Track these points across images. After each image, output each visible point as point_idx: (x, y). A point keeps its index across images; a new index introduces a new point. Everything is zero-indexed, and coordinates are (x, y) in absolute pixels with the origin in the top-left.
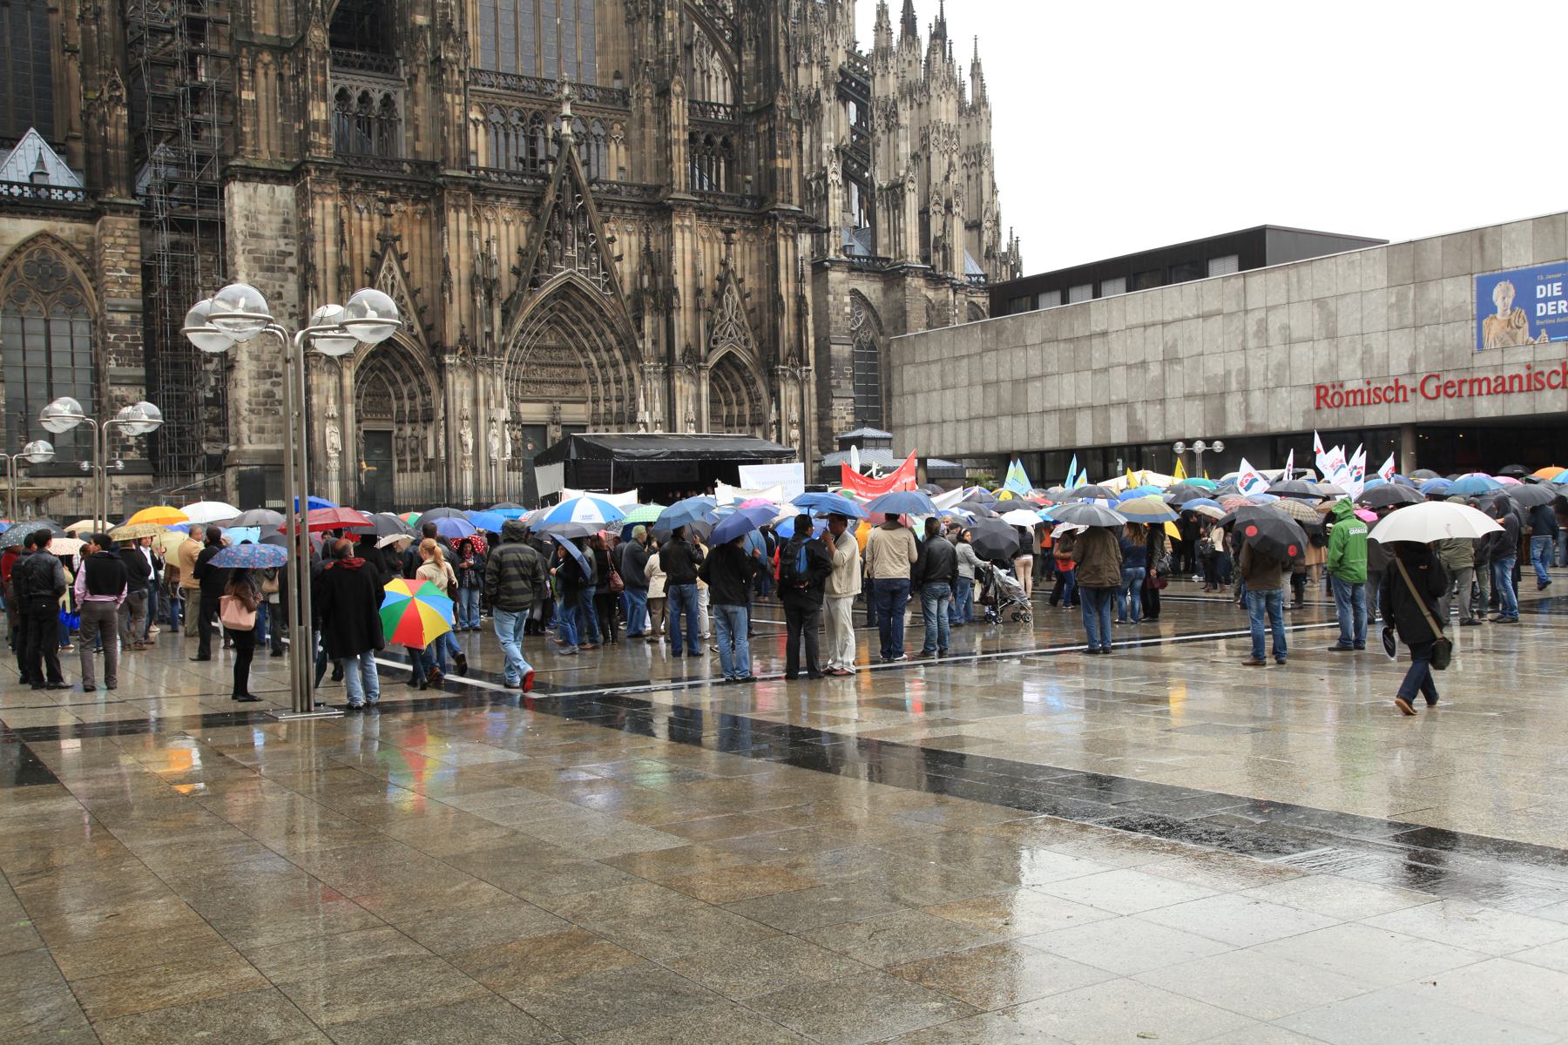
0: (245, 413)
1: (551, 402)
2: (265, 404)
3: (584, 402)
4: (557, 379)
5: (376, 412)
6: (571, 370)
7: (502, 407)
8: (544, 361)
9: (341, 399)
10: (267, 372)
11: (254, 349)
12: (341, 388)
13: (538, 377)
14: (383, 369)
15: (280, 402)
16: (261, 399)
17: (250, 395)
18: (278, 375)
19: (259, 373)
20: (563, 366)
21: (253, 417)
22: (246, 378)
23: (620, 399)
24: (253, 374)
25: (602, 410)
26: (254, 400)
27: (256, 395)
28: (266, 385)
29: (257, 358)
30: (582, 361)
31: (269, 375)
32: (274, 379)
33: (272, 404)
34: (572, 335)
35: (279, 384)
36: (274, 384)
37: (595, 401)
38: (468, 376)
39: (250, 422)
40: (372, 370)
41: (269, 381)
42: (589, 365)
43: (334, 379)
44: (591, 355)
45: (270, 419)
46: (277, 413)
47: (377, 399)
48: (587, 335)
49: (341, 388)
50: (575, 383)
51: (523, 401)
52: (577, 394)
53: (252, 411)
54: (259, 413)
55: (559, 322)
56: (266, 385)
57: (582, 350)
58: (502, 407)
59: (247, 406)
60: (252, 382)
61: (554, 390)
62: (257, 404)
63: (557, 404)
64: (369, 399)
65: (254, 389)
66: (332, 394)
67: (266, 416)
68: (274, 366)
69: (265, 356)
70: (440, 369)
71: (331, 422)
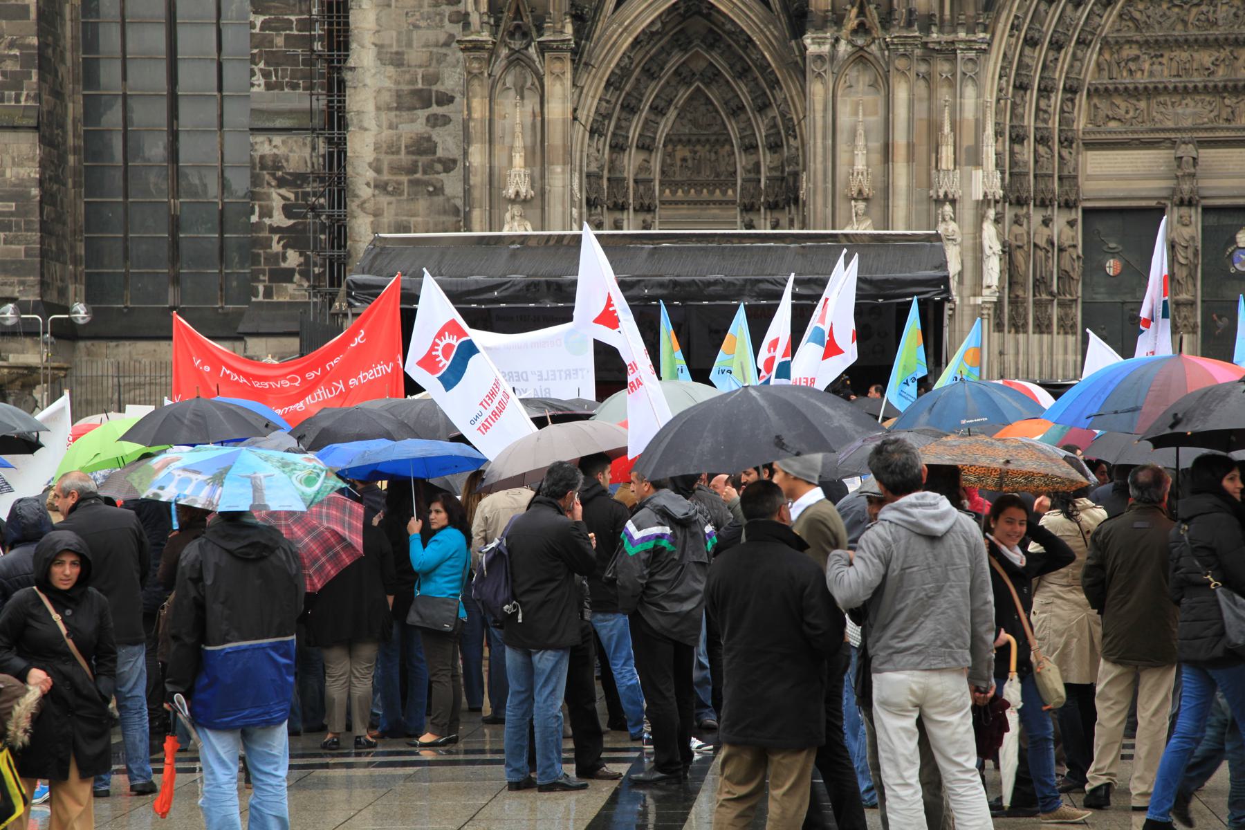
0: (365, 192)
1: (1173, 144)
2: (412, 170)
4: (1198, 79)
5: (692, 184)
7: (977, 162)
8: (1159, 33)
9: (539, 154)
10: (417, 93)
11: (390, 37)
12: (540, 124)
13: (1141, 79)
14: (713, 76)
15: (449, 165)
16: (404, 158)
17: (377, 148)
18: (447, 99)
19: (399, 95)
20: (1218, 43)
21: (384, 200)
22: (370, 107)
24: (386, 97)
26: (386, 160)
27: (393, 149)
28: (415, 125)
29: (397, 60)
31: (423, 99)
32: (435, 109)
33: (428, 169)
35: (446, 120)
36: (434, 121)
38: (873, 85)
39: (377, 214)
40: (682, 77)
41: (422, 114)
43: (531, 103)
45: (422, 204)
46: (438, 190)
47: (702, 151)
49: (540, 124)
51: (1091, 145)
53: (381, 187)
54: (397, 192)
56: (415, 125)
58: (977, 162)
59: (370, 175)
60: (384, 116)
61: (1188, 112)
62: (396, 169)
63: (1188, 151)
64: (680, 152)
65: (387, 134)
66: (519, 143)
67: (412, 198)
68: (433, 79)
69: (415, 56)
70: (799, 68)
71: (516, 210)
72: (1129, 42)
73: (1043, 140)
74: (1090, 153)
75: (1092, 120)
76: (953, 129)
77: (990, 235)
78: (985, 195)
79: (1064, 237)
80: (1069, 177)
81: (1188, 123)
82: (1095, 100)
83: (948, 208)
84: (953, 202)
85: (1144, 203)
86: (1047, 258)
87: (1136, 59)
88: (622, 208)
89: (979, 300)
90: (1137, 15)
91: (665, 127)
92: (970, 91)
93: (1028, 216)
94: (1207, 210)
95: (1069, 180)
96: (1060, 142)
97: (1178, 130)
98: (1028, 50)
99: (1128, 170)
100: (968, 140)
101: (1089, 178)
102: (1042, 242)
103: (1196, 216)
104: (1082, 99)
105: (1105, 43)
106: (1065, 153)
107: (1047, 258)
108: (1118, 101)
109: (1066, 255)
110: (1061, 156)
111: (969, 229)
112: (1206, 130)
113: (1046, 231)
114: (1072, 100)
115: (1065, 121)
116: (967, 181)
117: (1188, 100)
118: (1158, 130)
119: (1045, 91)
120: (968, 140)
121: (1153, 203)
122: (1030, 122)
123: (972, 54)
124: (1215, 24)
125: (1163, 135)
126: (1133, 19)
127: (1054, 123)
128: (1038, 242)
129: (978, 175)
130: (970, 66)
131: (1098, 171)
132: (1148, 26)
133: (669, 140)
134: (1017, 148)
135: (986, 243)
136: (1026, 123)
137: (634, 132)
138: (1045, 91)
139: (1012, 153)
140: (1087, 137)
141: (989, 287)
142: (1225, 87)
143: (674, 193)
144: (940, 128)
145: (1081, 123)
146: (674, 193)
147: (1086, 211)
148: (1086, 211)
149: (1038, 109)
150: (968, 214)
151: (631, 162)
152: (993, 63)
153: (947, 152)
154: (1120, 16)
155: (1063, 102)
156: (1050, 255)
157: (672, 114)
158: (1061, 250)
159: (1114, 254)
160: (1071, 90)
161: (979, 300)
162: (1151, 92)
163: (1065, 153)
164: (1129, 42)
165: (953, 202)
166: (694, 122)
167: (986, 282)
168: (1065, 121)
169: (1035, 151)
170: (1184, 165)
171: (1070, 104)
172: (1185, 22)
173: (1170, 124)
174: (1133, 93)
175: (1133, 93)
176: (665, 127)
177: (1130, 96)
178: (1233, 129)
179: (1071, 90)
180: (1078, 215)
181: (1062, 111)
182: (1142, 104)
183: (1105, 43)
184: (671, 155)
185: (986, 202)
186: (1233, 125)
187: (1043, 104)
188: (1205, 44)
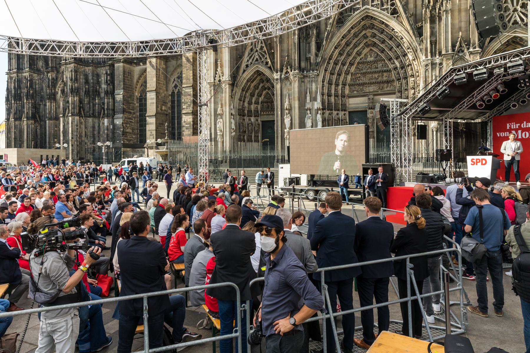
5: (266, 111)
6: (385, 74)
13: (361, 82)
30: (391, 66)
34: (383, 51)
42: (395, 68)
44: (395, 61)
48: (391, 49)
50: (388, 82)
55: (374, 45)
57: (390, 59)
61: (372, 88)
64: (265, 104)
72: (358, 73)
73: (336, 96)
74: (350, 99)
75: (350, 91)
76: (310, 93)
77: (319, 117)
81: (371, 90)
82: (351, 87)
83: (308, 112)
84: (310, 110)
85: (362, 109)
87: (360, 77)
88: (252, 116)
90: (359, 67)
91: (261, 99)
92: (314, 84)
93: (332, 113)
97: (370, 92)
98: (331, 76)
99: (359, 102)
100: (314, 96)
101: (350, 104)
102: (336, 119)
104: (347, 87)
105: (352, 74)
107: (338, 122)
108: (356, 87)
109: (343, 121)
110: (342, 100)
111: (314, 116)
112: (376, 92)
113: (337, 116)
114: (345, 87)
116: (313, 105)
118: (365, 93)
119: (337, 85)
120: (314, 96)
121: (364, 109)
122: (333, 92)
123: (314, 76)
124: (377, 68)
126: (358, 68)
127: (340, 92)
129: (316, 103)
130: (313, 79)
131: (352, 103)
132: (362, 70)
133: (262, 103)
134: (329, 98)
137: (253, 101)
138: (337, 85)
139: (328, 99)
142: (380, 82)
143: (264, 113)
144: (307, 93)
145: (347, 92)
146: (264, 113)
147: (350, 112)
148: (350, 112)
149: (335, 89)
150: (314, 112)
151: (253, 107)
152: (320, 78)
153: (308, 98)
154: (356, 68)
155: (342, 88)
157: (263, 97)
158: (342, 120)
160: (344, 85)
162: (363, 84)
164: (358, 73)
165: (310, 110)
166: (267, 98)
169: (335, 98)
172: (371, 68)
173: (368, 91)
174: (359, 85)
175: (359, 85)
176: (261, 99)
179: (344, 85)
180: (347, 113)
181: (342, 89)
182: (361, 87)
183: (352, 74)
184: (263, 105)
185: (318, 109)
187: (336, 88)
188: (375, 72)
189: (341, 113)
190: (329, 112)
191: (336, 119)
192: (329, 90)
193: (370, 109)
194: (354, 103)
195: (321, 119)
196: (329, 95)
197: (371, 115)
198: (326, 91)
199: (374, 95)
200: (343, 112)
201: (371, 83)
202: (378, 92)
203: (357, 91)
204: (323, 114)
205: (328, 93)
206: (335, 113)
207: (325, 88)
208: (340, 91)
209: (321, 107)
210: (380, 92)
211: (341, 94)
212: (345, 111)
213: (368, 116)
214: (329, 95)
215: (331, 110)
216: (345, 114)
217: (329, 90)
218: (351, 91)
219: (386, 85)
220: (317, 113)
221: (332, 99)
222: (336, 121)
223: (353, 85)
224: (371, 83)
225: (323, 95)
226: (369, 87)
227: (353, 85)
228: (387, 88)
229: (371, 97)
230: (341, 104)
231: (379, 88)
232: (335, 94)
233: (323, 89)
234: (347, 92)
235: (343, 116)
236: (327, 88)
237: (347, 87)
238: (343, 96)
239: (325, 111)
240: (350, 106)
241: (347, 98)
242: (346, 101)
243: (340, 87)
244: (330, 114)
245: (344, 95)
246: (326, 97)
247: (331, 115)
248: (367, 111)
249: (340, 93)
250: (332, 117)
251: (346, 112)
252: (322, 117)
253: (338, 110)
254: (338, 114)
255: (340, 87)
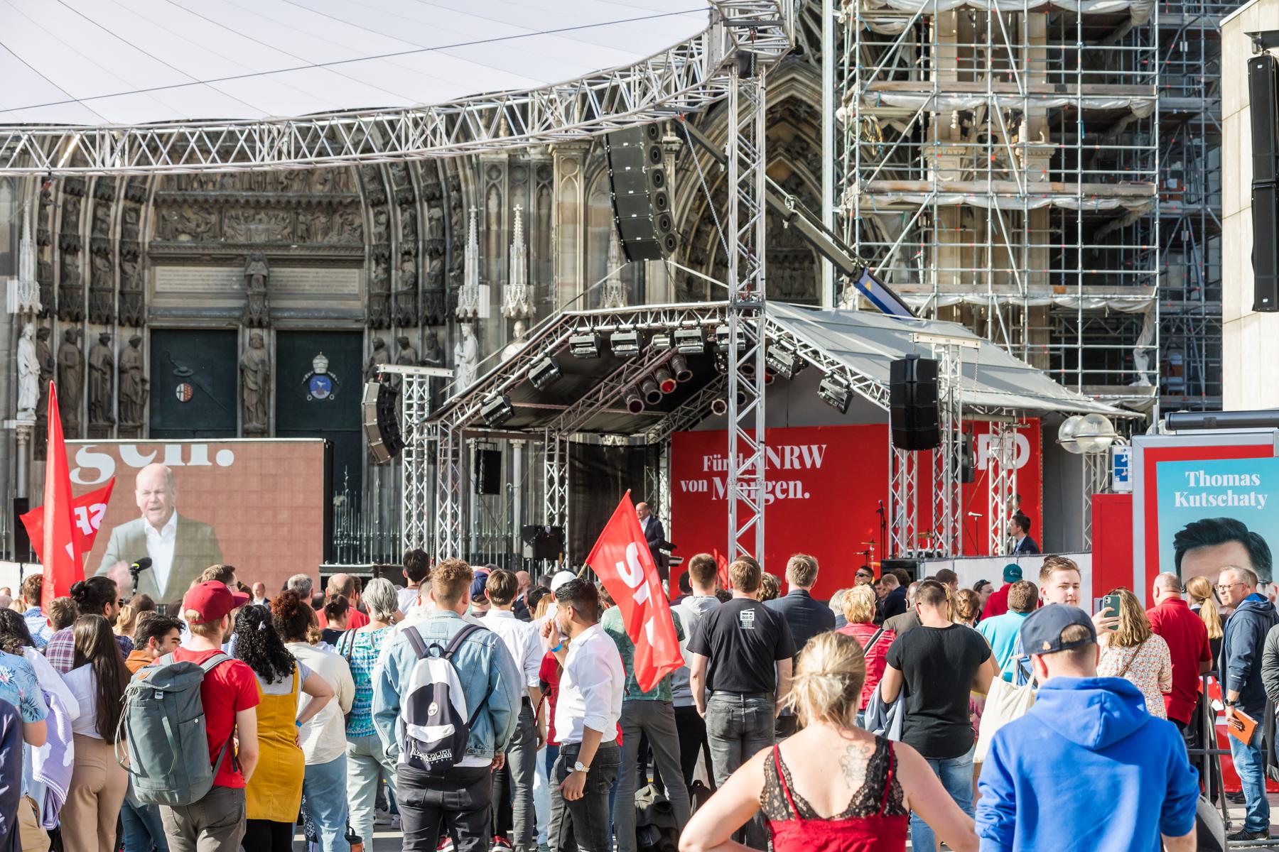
3: (358, 263)
4: (270, 194)
23: (435, 253)
25: (397, 284)
37: (383, 259)
52: (333, 238)
61: (260, 230)
73: (100, 251)
78: (21, 308)
79: (125, 358)
80: (131, 293)
81: (259, 239)
82: (165, 212)
86: (104, 380)
89: (12, 424)
93: (81, 333)
94: (281, 334)
95: (132, 297)
96: (121, 254)
97: (250, 246)
99: (200, 287)
101: (157, 294)
102: (98, 362)
103: (269, 338)
104: (148, 212)
106: (128, 267)
107: (104, 380)
108: (189, 213)
109: (127, 377)
112: (280, 247)
113: (103, 350)
114: (137, 211)
115: (128, 232)
117: (262, 215)
125: (234, 252)
127: (116, 234)
128: (94, 362)
129: (13, 285)
131: (168, 288)
134: (69, 259)
135: (21, 362)
136: (110, 236)
139: (63, 264)
140: (155, 251)
141: (25, 410)
142: (299, 203)
145: (146, 234)
147: (154, 331)
148: (154, 331)
149: (95, 218)
155: (125, 211)
156: (108, 377)
159: (183, 380)
161: (12, 424)
163: (128, 267)
167: (22, 403)
168: (128, 232)
169: (92, 262)
170: (254, 283)
171: (133, 215)
177: (202, 208)
178: (307, 248)
180: (145, 335)
181: (124, 221)
182: (214, 218)
185: (24, 316)
186: (308, 243)
187: (100, 213)
189: (122, 335)
190: (66, 326)
191: (98, 362)
192: (69, 222)
193: (251, 324)
194: (176, 288)
195: (35, 366)
196: (69, 248)
197: (257, 355)
198: (55, 227)
199: (274, 261)
200: (127, 333)
201: (258, 206)
202: (287, 247)
203: (195, 236)
204: (42, 335)
205: (62, 237)
206: (93, 331)
207: (50, 209)
208: (118, 229)
209: (38, 307)
210: (295, 250)
211: (122, 243)
212: (137, 324)
213: (242, 358)
214: (69, 248)
215: (77, 318)
216: (135, 343)
217: (69, 222)
218: (162, 226)
219: (323, 220)
220: (20, 334)
221: (82, 263)
222: (96, 374)
223: (174, 203)
224: (258, 206)
225: (42, 243)
226: (246, 220)
227: (174, 203)
228: (326, 234)
229: (258, 269)
230: (122, 293)
231: (294, 232)
232: (93, 240)
233: (43, 218)
234: (146, 234)
235: (130, 353)
236: (59, 212)
237: (148, 212)
238: (130, 255)
239: (46, 324)
240: (161, 303)
241: (148, 261)
242: (142, 279)
243: (116, 210)
244: (69, 338)
245: (133, 247)
246: (53, 256)
247: (74, 343)
248: (234, 333)
249: (118, 236)
250: (81, 352)
251: (139, 333)
252: (39, 355)
253: (108, 321)
254: (104, 340)
255: (116, 209)
